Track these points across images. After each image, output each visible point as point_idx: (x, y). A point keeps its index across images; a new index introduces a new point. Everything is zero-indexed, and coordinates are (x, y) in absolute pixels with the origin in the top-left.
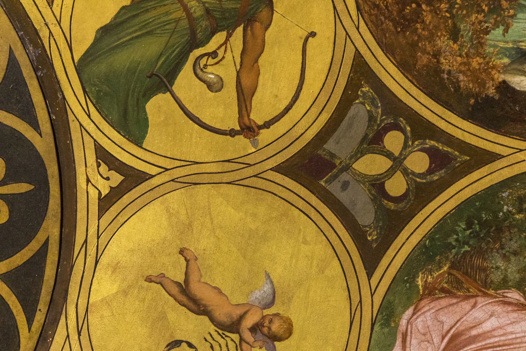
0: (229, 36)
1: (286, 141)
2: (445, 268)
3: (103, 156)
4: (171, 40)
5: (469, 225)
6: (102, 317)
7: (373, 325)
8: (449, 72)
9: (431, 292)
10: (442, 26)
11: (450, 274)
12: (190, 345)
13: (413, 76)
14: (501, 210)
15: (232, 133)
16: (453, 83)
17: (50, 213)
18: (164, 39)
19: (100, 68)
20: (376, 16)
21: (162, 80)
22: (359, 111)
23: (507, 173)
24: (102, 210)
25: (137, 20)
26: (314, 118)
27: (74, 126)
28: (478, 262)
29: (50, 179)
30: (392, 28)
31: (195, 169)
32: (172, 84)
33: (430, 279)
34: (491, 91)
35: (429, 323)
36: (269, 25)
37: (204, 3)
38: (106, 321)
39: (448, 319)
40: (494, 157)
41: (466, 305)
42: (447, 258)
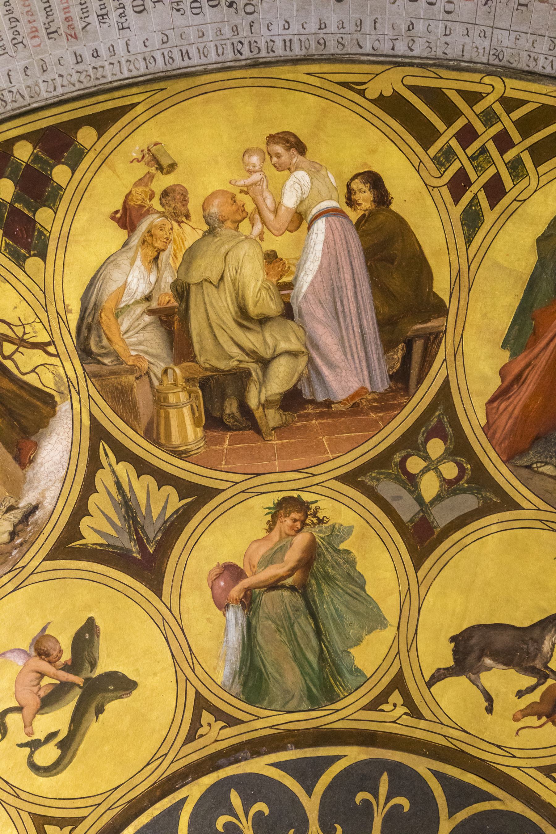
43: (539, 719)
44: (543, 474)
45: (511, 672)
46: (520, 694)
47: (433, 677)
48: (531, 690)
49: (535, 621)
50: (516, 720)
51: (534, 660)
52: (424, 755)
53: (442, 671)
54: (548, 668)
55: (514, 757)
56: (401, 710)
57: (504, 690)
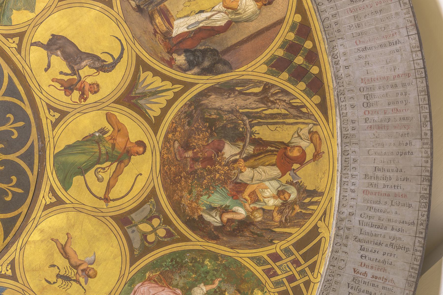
0: (112, 164)
1: (118, 208)
2: (158, 273)
3: (52, 190)
4: (91, 159)
5: (172, 261)
7: (125, 284)
8: (184, 205)
9: (150, 279)
10: (187, 188)
11: (159, 276)
12: (58, 268)
13: (171, 202)
14: (185, 260)
15: (100, 199)
17: (26, 203)
18: (88, 157)
19: (63, 159)
20: (165, 176)
21: (83, 171)
22: (148, 207)
23: (191, 248)
24: (45, 209)
25: (81, 147)
26: (131, 203)
27: (45, 176)
28: (170, 275)
30: (169, 182)
31: (82, 206)
32: (85, 173)
33: (151, 275)
34: (196, 217)
35: (145, 291)
37: (107, 150)
38: (32, 249)
40: (188, 240)
41: (161, 289)
42: (160, 270)
43: (61, 87)
44: (130, 3)
46: (61, 73)
47: (35, 43)
48: (66, 74)
49: (87, 52)
50: (53, 80)
51: (75, 65)
52: (11, 68)
53: (40, 43)
55: (42, 93)
56: (14, 45)
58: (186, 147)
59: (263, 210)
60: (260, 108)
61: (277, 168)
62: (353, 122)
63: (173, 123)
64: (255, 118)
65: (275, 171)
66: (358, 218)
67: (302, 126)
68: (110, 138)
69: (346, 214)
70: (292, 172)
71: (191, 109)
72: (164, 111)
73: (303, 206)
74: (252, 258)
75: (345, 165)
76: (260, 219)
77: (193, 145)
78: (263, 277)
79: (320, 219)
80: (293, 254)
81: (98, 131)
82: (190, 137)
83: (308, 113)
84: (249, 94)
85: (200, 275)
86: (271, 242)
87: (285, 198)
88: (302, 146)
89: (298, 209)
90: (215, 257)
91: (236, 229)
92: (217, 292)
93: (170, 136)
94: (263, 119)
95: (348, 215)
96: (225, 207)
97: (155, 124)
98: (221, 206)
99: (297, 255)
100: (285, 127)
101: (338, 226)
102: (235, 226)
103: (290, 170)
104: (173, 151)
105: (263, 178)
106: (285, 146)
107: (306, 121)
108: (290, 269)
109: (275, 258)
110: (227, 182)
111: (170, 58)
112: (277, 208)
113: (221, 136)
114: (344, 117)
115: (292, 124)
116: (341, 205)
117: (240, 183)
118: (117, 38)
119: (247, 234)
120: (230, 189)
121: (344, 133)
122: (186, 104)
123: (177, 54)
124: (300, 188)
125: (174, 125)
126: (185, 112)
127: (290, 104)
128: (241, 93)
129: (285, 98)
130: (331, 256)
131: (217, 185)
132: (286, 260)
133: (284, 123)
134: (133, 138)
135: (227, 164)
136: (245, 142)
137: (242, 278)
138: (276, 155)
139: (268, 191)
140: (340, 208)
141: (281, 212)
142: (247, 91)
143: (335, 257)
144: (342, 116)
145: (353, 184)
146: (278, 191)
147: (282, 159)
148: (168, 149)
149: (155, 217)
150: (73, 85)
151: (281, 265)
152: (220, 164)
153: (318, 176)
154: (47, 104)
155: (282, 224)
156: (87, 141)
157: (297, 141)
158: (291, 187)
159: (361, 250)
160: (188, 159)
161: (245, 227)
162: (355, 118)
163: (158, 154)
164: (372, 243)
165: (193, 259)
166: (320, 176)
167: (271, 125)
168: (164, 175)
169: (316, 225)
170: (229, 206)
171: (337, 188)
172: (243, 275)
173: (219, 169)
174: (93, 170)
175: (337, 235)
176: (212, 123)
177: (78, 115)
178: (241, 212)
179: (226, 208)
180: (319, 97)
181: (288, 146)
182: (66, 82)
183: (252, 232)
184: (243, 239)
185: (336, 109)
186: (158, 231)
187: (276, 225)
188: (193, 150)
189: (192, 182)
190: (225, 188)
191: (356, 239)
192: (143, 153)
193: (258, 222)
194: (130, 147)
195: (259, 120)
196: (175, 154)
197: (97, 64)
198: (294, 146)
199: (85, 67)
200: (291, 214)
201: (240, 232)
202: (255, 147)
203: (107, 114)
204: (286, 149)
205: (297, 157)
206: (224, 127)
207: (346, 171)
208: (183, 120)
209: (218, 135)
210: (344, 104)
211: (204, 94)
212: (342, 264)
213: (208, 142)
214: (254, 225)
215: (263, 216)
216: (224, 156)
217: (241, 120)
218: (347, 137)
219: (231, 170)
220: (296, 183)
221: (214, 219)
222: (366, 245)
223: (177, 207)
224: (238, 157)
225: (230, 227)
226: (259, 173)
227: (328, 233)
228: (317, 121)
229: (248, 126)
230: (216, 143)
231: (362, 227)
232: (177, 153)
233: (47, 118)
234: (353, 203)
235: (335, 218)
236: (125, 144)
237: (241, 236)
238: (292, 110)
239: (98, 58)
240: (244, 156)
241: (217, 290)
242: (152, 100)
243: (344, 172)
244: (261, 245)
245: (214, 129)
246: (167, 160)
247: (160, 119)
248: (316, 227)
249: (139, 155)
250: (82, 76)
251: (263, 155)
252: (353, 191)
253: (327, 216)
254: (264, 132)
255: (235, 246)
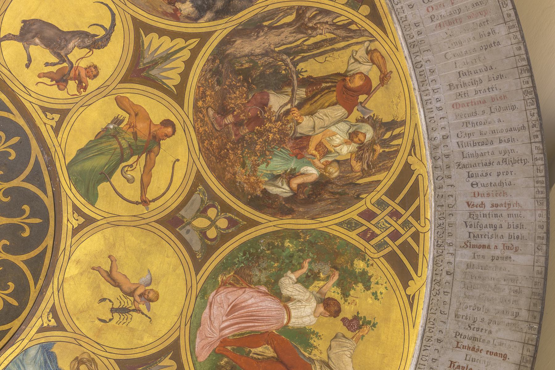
0: (139, 158)
2: (232, 274)
3: (76, 209)
4: (112, 158)
5: (245, 254)
6: (70, 284)
8: (240, 183)
9: (224, 284)
10: (238, 161)
11: (234, 276)
12: (110, 301)
15: (137, 203)
16: (241, 188)
17: (49, 234)
18: (108, 157)
19: (78, 168)
20: (208, 154)
21: (106, 175)
22: (197, 197)
24: (74, 235)
25: (96, 148)
27: (63, 194)
28: (247, 272)
29: (50, 218)
30: (215, 160)
32: (111, 178)
33: (224, 278)
34: (259, 193)
35: (223, 299)
36: (158, 154)
38: (71, 286)
39: (232, 298)
40: (257, 223)
41: (240, 291)
42: (233, 269)
43: (51, 81)
45: (47, 51)
46: (47, 64)
47: (5, 36)
48: (54, 64)
50: (39, 76)
51: (61, 50)
53: (11, 36)
54: (66, 56)
55: (30, 95)
57: (40, 59)
58: (223, 111)
59: (338, 161)
60: (299, 39)
61: (341, 107)
62: (416, 25)
63: (199, 87)
64: (297, 53)
65: (339, 111)
66: (455, 140)
67: (356, 48)
68: (128, 126)
69: (439, 139)
70: (360, 106)
71: (216, 65)
72: (185, 76)
73: (385, 143)
74: (340, 224)
75: (421, 80)
76: (336, 174)
77: (232, 107)
78: (360, 243)
79: (410, 154)
80: (389, 205)
81: (112, 122)
82: (224, 99)
83: (360, 30)
84: (282, 26)
85: (283, 263)
86: (358, 198)
87: (359, 140)
88: (363, 72)
89: (379, 149)
90: (295, 235)
91: (311, 194)
92: (309, 276)
93: (200, 104)
94: (307, 52)
95: (442, 139)
96: (290, 171)
97: (178, 95)
98: (286, 171)
99: (394, 205)
100: (336, 54)
101: (433, 155)
102: (310, 191)
103: (356, 105)
104: (208, 122)
105: (327, 123)
106: (343, 78)
107: (360, 40)
108: (389, 224)
109: (368, 215)
110: (285, 140)
111: (173, 9)
112: (354, 155)
113: (262, 87)
114: (404, 23)
115: (343, 48)
116: (430, 129)
117: (301, 137)
118: (102, 3)
119: (326, 196)
120: (291, 148)
121: (410, 41)
122: (208, 60)
123: (180, 2)
124: (375, 123)
125: (201, 89)
126: (211, 70)
127: (334, 24)
128: (271, 28)
129: (326, 19)
130: (435, 194)
131: (274, 147)
132: (382, 215)
133: (333, 50)
134: (157, 119)
135: (279, 119)
136: (293, 86)
137: (335, 252)
138: (334, 91)
139: (337, 138)
140: (429, 133)
141: (360, 158)
142: (278, 24)
143: (440, 194)
144: (401, 21)
145: (438, 100)
146: (350, 134)
147: (344, 93)
148: (202, 121)
149: (209, 207)
150: (65, 76)
151: (378, 223)
152: (270, 121)
153: (392, 102)
154: (41, 107)
155: (365, 173)
156: (101, 138)
157: (355, 67)
158: (364, 124)
159: (469, 177)
160: (230, 125)
161: (322, 189)
162: (418, 20)
163: (191, 129)
164: (481, 165)
165: (269, 244)
166: (395, 102)
167: (318, 56)
168: (206, 152)
169: (407, 162)
170: (295, 169)
171: (419, 111)
172: (335, 247)
173: (270, 127)
174: (119, 171)
175: (435, 167)
176: (246, 74)
177: (81, 109)
178: (311, 172)
179: (292, 172)
180: (367, 7)
181: (347, 76)
182: (55, 73)
183: (332, 193)
184: (323, 203)
185: (391, 16)
186: (217, 223)
187: (359, 176)
188: (233, 113)
189: (243, 152)
190: (283, 148)
191: (459, 165)
192: (174, 133)
193: (336, 178)
194: (156, 131)
195: (302, 54)
196: (212, 124)
197: (88, 42)
198: (354, 75)
199: (73, 49)
200: (373, 158)
201: (317, 197)
202: (307, 89)
203: (116, 99)
204: (344, 80)
205: (361, 87)
206: (262, 75)
207: (425, 86)
208: (210, 81)
209: (257, 87)
210: (399, 6)
211: (227, 41)
212: (451, 201)
213: (248, 98)
214: (331, 183)
215: (340, 169)
216: (272, 110)
217: (280, 61)
218: (414, 46)
219: (286, 125)
220: (368, 118)
221: (281, 190)
222: (473, 170)
223: (233, 187)
224: (289, 106)
225: (303, 193)
226: (320, 119)
227: (424, 168)
228: (372, 36)
229: (291, 66)
230: (259, 97)
231: (462, 149)
232: (215, 123)
233: (45, 124)
234: (443, 123)
235: (427, 148)
236: (148, 130)
237: (320, 201)
238: (338, 32)
239: (86, 35)
240: (296, 103)
241: (309, 274)
242: (166, 67)
243: (423, 89)
244: (346, 205)
245: (250, 81)
246: (205, 134)
247: (182, 87)
248: (407, 165)
249: (169, 137)
250: (73, 61)
251: (319, 96)
252: (440, 109)
253: (417, 148)
254: (312, 68)
255: (316, 215)
